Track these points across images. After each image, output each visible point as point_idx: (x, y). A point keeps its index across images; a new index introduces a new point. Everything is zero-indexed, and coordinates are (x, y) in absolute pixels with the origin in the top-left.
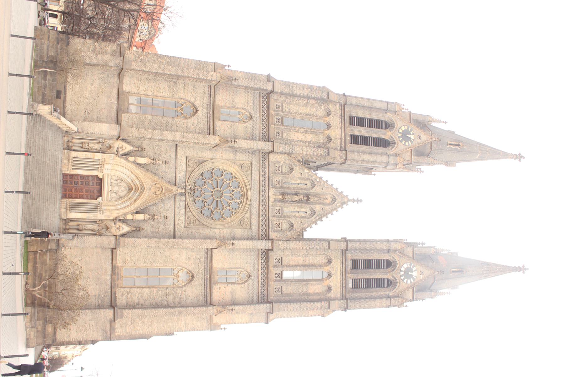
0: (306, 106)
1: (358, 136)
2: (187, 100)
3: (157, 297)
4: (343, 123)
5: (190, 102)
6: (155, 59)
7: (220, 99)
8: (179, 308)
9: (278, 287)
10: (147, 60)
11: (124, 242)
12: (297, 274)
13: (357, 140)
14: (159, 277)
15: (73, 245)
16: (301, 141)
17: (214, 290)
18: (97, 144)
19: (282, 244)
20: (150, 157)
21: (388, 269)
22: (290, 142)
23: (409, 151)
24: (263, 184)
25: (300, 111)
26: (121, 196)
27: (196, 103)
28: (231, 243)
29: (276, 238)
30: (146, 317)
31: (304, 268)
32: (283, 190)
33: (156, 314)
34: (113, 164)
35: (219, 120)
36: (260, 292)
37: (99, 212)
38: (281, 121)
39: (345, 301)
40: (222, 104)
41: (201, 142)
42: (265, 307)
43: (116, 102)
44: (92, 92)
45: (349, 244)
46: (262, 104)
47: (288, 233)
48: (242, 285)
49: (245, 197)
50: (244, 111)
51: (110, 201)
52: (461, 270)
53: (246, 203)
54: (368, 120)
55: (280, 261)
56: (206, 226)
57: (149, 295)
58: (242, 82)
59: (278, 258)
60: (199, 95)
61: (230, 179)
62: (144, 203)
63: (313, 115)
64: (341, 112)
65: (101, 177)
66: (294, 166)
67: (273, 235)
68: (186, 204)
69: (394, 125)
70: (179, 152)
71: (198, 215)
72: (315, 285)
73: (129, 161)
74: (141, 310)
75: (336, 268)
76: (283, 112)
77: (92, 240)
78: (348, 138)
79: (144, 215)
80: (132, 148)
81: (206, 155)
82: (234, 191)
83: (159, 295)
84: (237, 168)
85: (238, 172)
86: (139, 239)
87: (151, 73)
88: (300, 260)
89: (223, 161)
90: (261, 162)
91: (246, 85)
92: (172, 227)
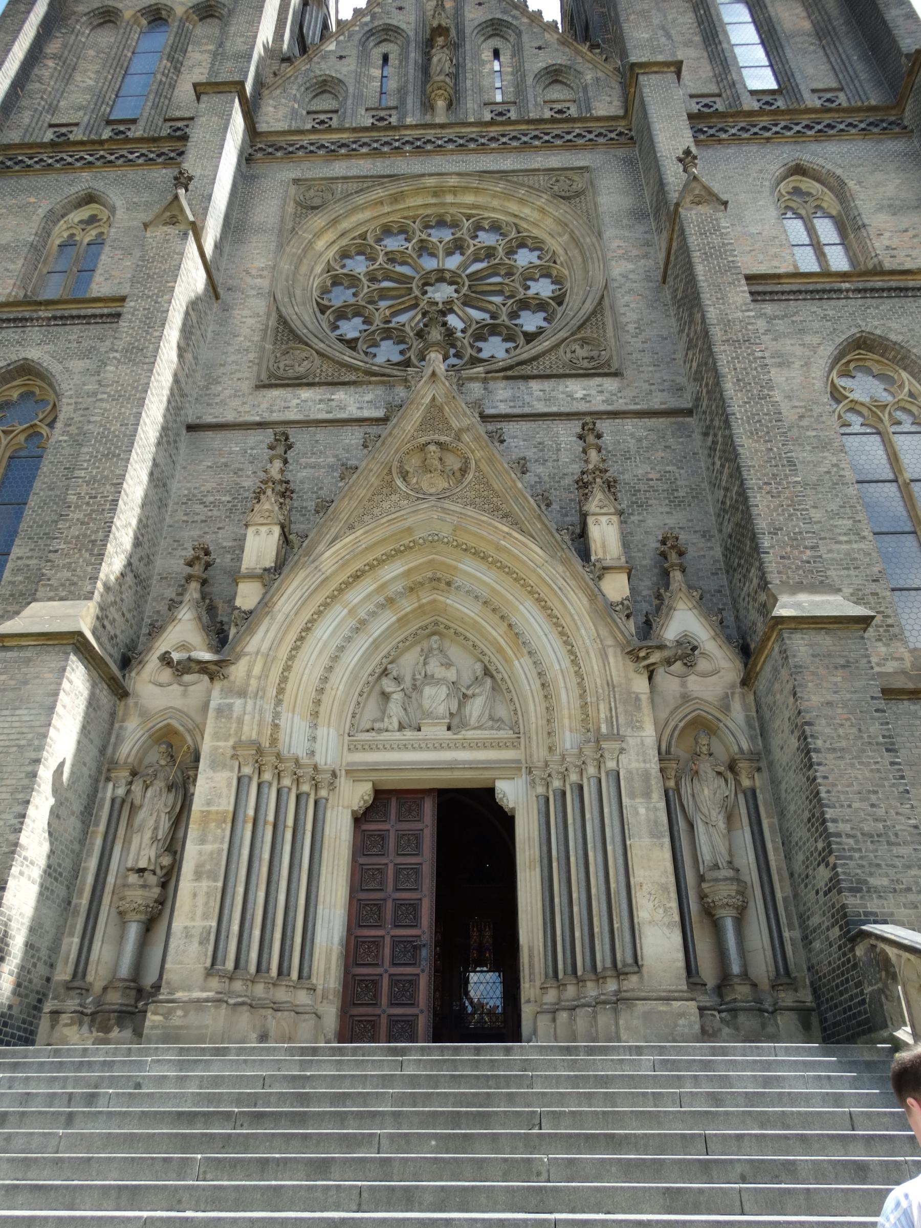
18: (142, 814)
26: (479, 672)
34: (279, 702)
37: (611, 765)
47: (589, 77)
48: (851, 184)
51: (515, 727)
56: (600, 303)
68: (502, 374)
70: (230, 416)
73: (265, 605)
79: (590, 520)
82: (424, 236)
84: (318, 221)
86: (754, 511)
92: (629, 425)
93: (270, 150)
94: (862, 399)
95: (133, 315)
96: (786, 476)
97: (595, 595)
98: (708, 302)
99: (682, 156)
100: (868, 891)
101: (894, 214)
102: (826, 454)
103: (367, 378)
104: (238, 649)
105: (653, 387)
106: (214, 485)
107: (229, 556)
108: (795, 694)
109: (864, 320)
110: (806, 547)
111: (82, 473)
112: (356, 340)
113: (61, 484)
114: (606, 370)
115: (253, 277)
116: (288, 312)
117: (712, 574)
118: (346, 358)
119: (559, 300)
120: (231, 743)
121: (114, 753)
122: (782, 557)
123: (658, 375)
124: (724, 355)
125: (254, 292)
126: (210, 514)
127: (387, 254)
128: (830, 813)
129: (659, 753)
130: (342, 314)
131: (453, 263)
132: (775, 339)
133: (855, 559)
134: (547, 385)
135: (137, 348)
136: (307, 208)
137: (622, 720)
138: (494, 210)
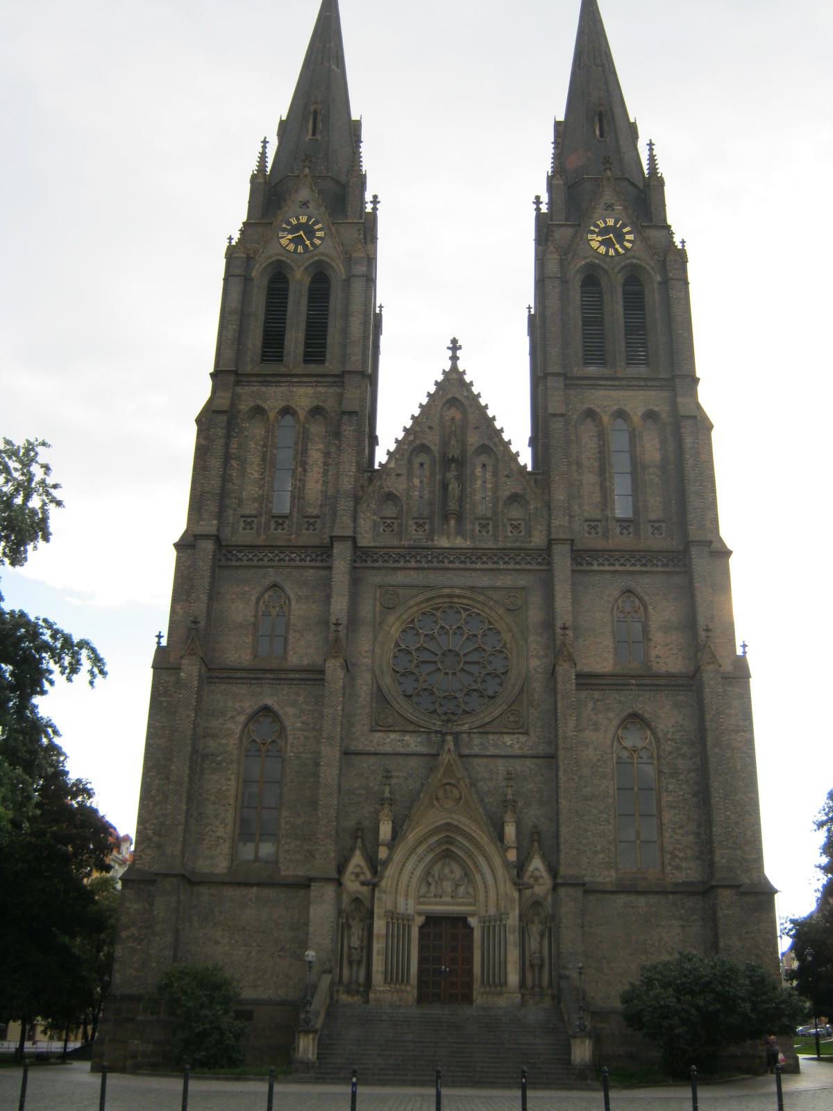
0: (243, 462)
1: (307, 346)
2: (243, 731)
3: (681, 793)
4: (279, 379)
5: (247, 724)
6: (151, 804)
7: (237, 655)
8: (708, 747)
9: (650, 530)
10: (155, 822)
12: (621, 486)
13: (315, 349)
14: (636, 789)
16: (325, 473)
18: (353, 930)
19: (559, 521)
20: (377, 812)
21: (603, 284)
22: (330, 500)
23: (336, 230)
24: (424, 560)
25: (256, 475)
27: (249, 711)
28: (561, 632)
29: (545, 532)
30: (728, 818)
31: (607, 470)
32: (436, 517)
33: (722, 796)
34: (396, 894)
35: (286, 659)
36: (662, 569)
37: (504, 923)
38: (280, 520)
39: (677, 380)
40: (249, 651)
41: (341, 699)
42: (699, 562)
43: (255, 889)
44: (233, 942)
45: (551, 370)
46: (246, 563)
47: (532, 507)
48: (650, 608)
49: (456, 600)
50: (262, 601)
51: (475, 897)
52: (596, 118)
53: (469, 598)
54: (267, 321)
55: (593, 524)
57: (677, 811)
58: (199, 608)
59: (587, 528)
60: (230, 704)
61: (416, 634)
63: (263, 448)
64: (255, 384)
66: (382, 490)
67: (538, 539)
68: (475, 731)
69: (279, 261)
70: (361, 747)
71: (501, 705)
72: (643, 447)
74: (714, 829)
75: (605, 400)
76: (261, 515)
77: (569, 936)
78: (313, 368)
79: (506, 824)
81: (365, 688)
82: (443, 625)
83: (677, 790)
84: (391, 619)
85: (401, 615)
87: (188, 814)
88: (590, 478)
89: (378, 651)
90: (376, 565)
91: (204, 598)
92: (528, 762)
95: (328, 717)
103: (417, 729)
118: (410, 716)
119: (505, 673)
120: (384, 910)
125: (364, 668)
128: (561, 946)
132: (596, 714)
134: (496, 737)
136: (386, 608)
138: (477, 608)
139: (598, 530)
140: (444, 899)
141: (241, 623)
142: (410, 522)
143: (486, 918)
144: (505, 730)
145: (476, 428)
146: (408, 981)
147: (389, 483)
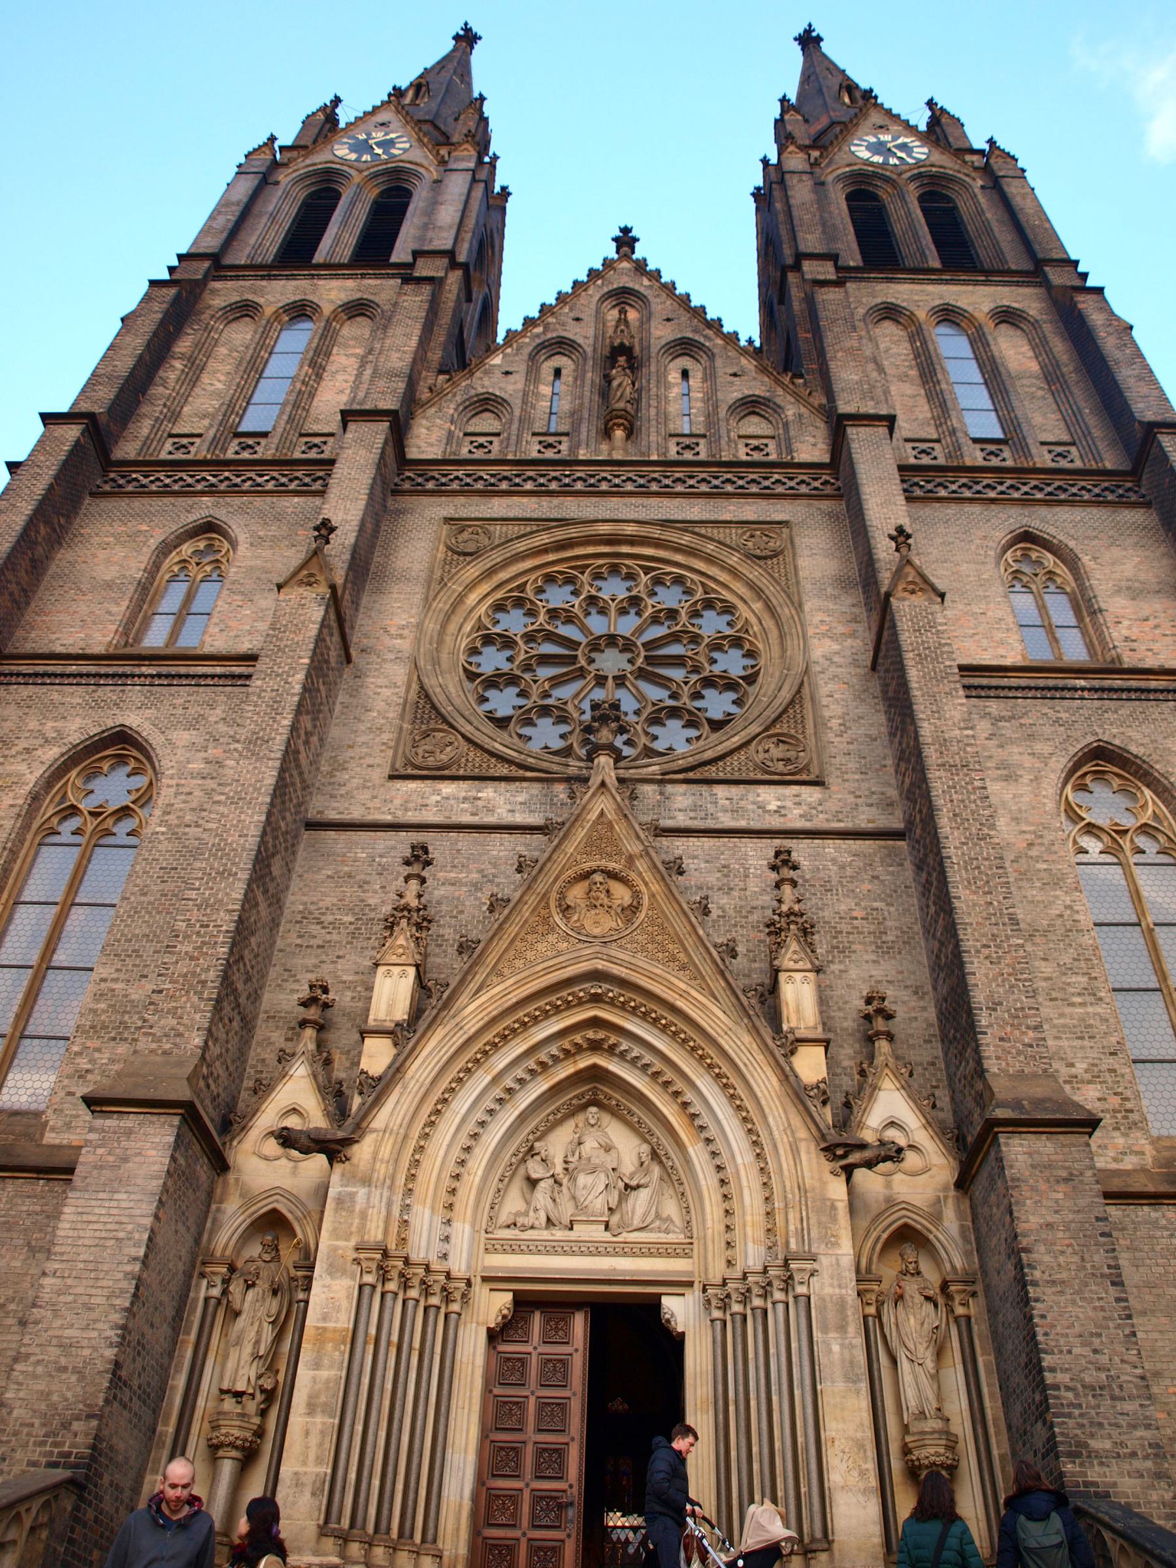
11: (1020, 1075)
15: (1154, 1496)
16: (359, 375)
17: (1150, 662)
18: (241, 1322)
27: (75, 738)
37: (801, 1289)
40: (114, 627)
47: (790, 413)
48: (1086, 559)
49: (625, 549)
53: (658, 544)
56: (799, 691)
62: (698, 976)
65: (504, 1300)
68: (680, 776)
70: (356, 813)
73: (397, 1070)
79: (782, 977)
80: (300, 1071)
82: (594, 592)
86: (971, 980)
92: (831, 847)
93: (420, 480)
94: (1099, 822)
95: (259, 696)
96: (1008, 937)
97: (788, 1077)
98: (921, 716)
99: (895, 533)
100: (1089, 1457)
101: (1133, 599)
102: (1058, 893)
103: (521, 773)
104: (364, 1125)
105: (859, 801)
106: (335, 900)
107: (349, 994)
108: (1011, 1213)
109: (1101, 726)
110: (1028, 1027)
111: (193, 894)
112: (508, 719)
113: (156, 888)
114: (804, 777)
115: (392, 637)
116: (431, 683)
117: (926, 1041)
119: (751, 679)
120: (353, 1243)
121: (210, 1240)
122: (1001, 1039)
123: (865, 785)
124: (938, 780)
125: (391, 656)
126: (328, 937)
127: (549, 611)
129: (858, 1271)
130: (494, 682)
131: (626, 626)
132: (1001, 746)
133: (1090, 1026)
134: (735, 791)
135: (262, 739)
136: (459, 554)
137: (814, 1233)
139: (935, 454)
140: (581, 1232)
141: (113, 581)
142: (527, 436)
143: (731, 1286)
144: (760, 776)
145: (668, 320)
146: (430, 1537)
147: (486, 382)
